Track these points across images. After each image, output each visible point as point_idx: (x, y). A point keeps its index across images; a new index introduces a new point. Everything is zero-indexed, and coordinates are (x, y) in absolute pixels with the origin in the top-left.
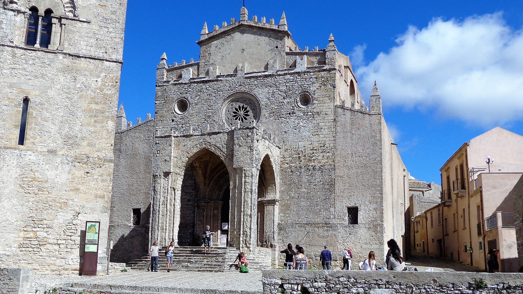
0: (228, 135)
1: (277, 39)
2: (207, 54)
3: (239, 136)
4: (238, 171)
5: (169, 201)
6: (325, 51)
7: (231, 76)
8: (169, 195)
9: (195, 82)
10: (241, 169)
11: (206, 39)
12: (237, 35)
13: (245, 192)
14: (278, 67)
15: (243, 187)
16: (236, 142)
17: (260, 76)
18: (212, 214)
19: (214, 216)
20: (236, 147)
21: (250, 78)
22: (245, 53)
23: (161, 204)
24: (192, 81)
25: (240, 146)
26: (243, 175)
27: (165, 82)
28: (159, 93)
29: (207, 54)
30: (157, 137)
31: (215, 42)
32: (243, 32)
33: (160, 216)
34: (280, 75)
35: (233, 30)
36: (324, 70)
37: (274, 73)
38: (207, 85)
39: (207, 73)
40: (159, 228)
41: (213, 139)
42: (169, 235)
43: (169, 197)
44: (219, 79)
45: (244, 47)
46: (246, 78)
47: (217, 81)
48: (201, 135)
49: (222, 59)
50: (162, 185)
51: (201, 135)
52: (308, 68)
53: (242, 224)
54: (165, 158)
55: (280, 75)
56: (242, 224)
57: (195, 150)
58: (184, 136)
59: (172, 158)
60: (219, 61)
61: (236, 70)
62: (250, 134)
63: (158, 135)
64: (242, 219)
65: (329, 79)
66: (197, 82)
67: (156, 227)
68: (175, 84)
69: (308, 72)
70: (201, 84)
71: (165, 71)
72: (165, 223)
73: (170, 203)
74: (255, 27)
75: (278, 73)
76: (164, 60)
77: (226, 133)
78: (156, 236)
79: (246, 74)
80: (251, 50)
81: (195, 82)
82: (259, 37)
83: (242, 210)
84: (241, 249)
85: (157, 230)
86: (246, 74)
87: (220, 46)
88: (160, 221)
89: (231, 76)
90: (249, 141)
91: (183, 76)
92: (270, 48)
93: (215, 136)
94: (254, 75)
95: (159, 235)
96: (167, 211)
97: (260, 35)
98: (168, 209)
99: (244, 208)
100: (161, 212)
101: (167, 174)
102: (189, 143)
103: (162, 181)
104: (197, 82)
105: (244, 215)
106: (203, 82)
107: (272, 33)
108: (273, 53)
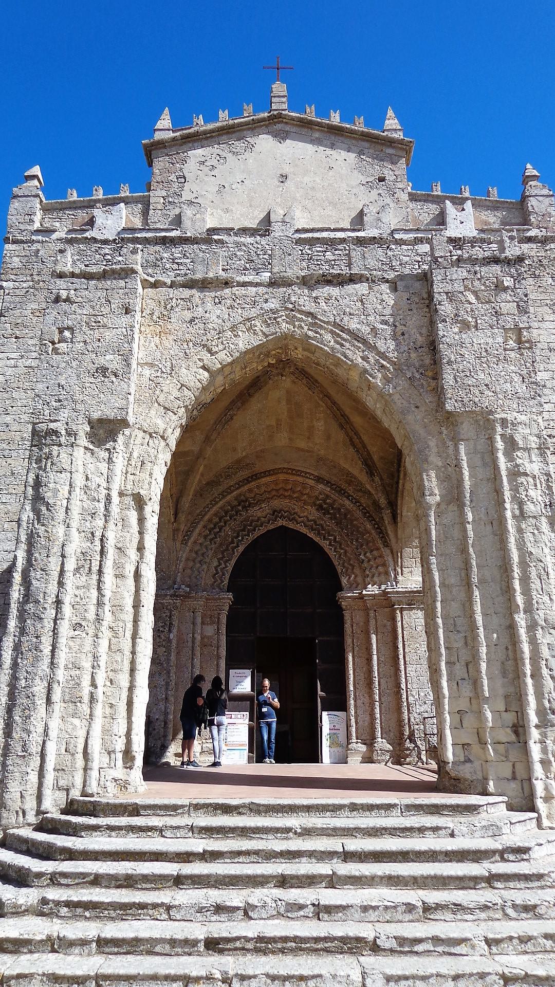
0: (394, 289)
1: (382, 160)
2: (173, 177)
3: (458, 287)
4: (466, 428)
5: (111, 553)
6: (524, 198)
7: (252, 232)
8: (111, 525)
9: (135, 241)
10: (484, 421)
11: (174, 139)
12: (264, 142)
13: (522, 516)
14: (392, 220)
15: (507, 494)
16: (446, 308)
17: (343, 241)
18: (198, 637)
19: (204, 645)
20: (448, 333)
21: (312, 242)
22: (288, 183)
23: (70, 565)
24: (126, 238)
25: (465, 326)
26: (500, 445)
27: (38, 232)
28: (16, 259)
29: (173, 177)
30: (61, 276)
31: (200, 151)
32: (281, 136)
33: (65, 629)
34: (400, 242)
35: (255, 127)
36: (530, 240)
37: (385, 236)
38: (177, 252)
39: (178, 221)
40: (57, 696)
41: (331, 302)
42: (106, 731)
43: (111, 535)
44: (215, 237)
45: (287, 170)
46: (299, 242)
47: (208, 241)
48: (272, 284)
49: (219, 192)
50: (79, 481)
51: (272, 284)
52: (482, 231)
53: (528, 670)
54: (101, 361)
55: (400, 242)
56: (528, 670)
57: (244, 342)
58: (190, 284)
59: (134, 366)
60: (210, 197)
61: (267, 220)
62: (508, 282)
63: (69, 268)
64: (526, 648)
65: (545, 262)
66: (146, 241)
67: (39, 688)
68: (70, 241)
69: (483, 241)
70: (157, 248)
71: (39, 206)
72: (87, 664)
73: (118, 566)
74: (319, 124)
75: (397, 236)
76: (36, 182)
77: (387, 281)
78: (35, 739)
79: (297, 231)
80: (306, 179)
81: (135, 241)
82: (329, 151)
83: (520, 600)
84: (540, 804)
85: (41, 702)
86: (297, 231)
87: (215, 162)
88: (63, 657)
89: (252, 232)
90: (508, 306)
91: (99, 221)
92: (364, 180)
93: (334, 291)
94: (325, 235)
95: (53, 733)
96: (100, 604)
97: (332, 146)
98: (108, 593)
99: (527, 592)
100: (67, 610)
101: (105, 431)
102: (213, 310)
103: (79, 462)
104: (146, 241)
105: (532, 627)
106: (164, 241)
107: (367, 145)
108: (375, 192)
